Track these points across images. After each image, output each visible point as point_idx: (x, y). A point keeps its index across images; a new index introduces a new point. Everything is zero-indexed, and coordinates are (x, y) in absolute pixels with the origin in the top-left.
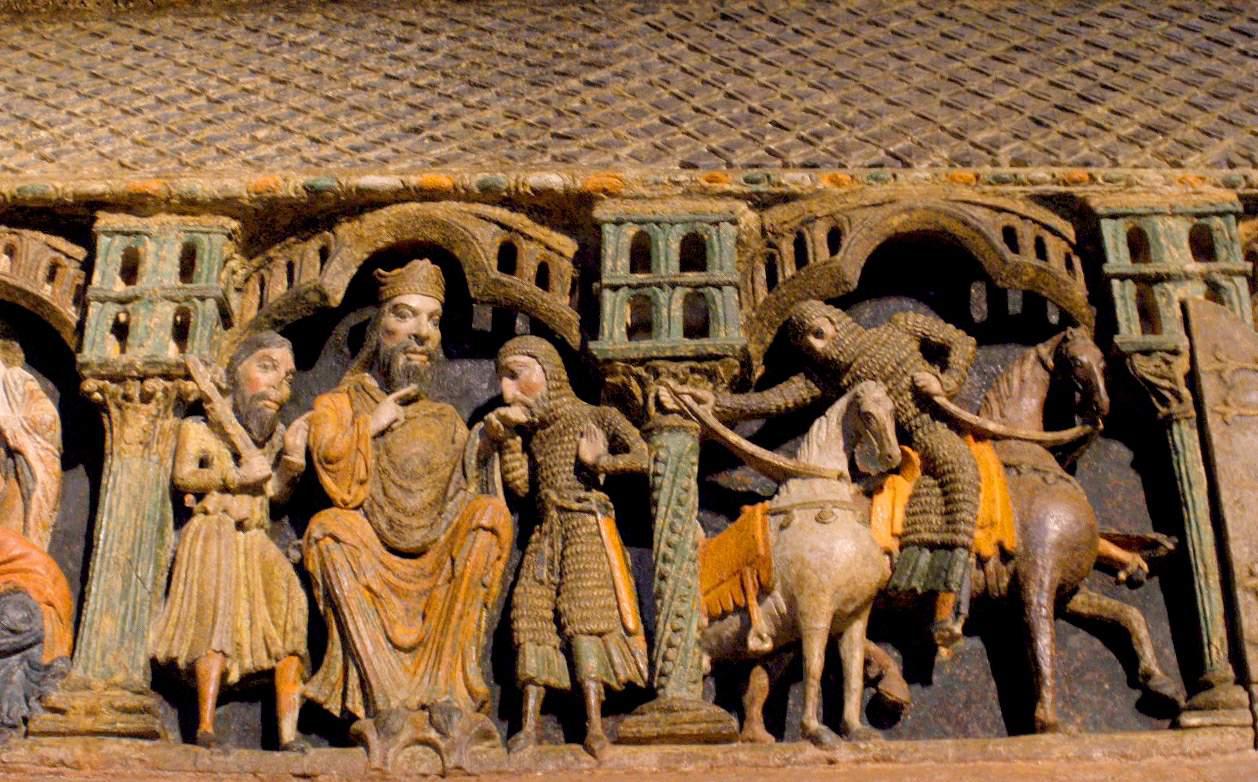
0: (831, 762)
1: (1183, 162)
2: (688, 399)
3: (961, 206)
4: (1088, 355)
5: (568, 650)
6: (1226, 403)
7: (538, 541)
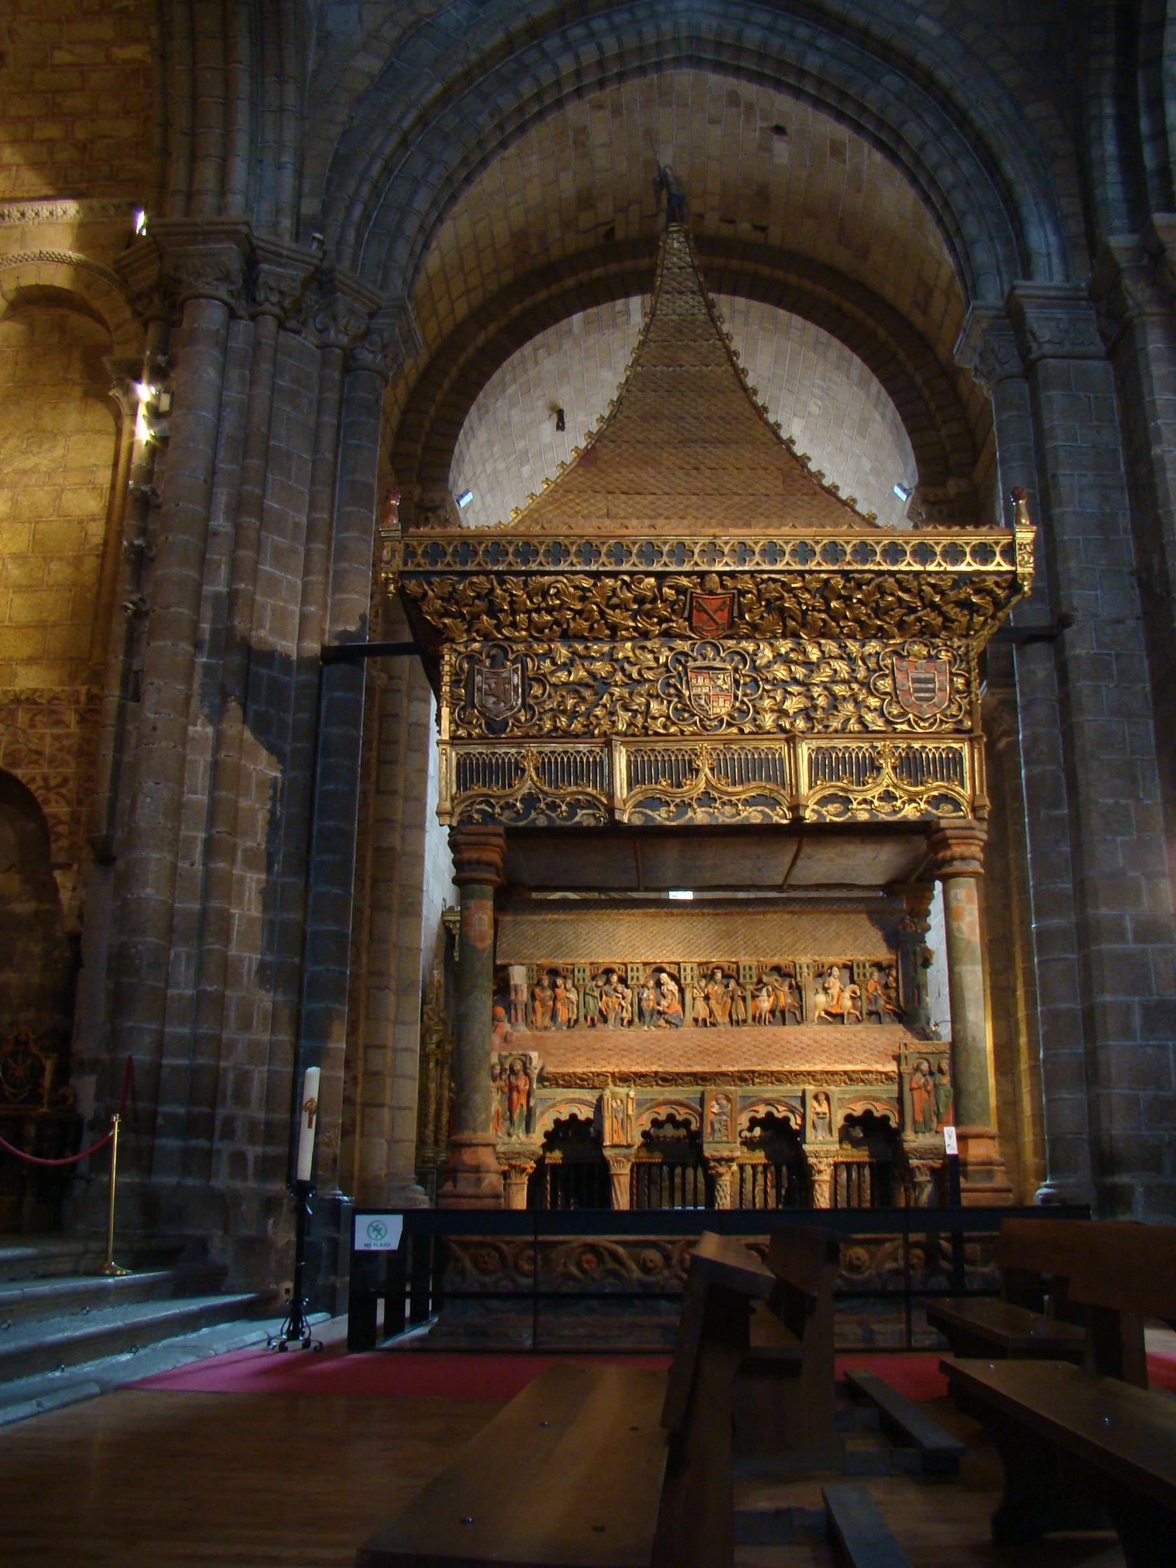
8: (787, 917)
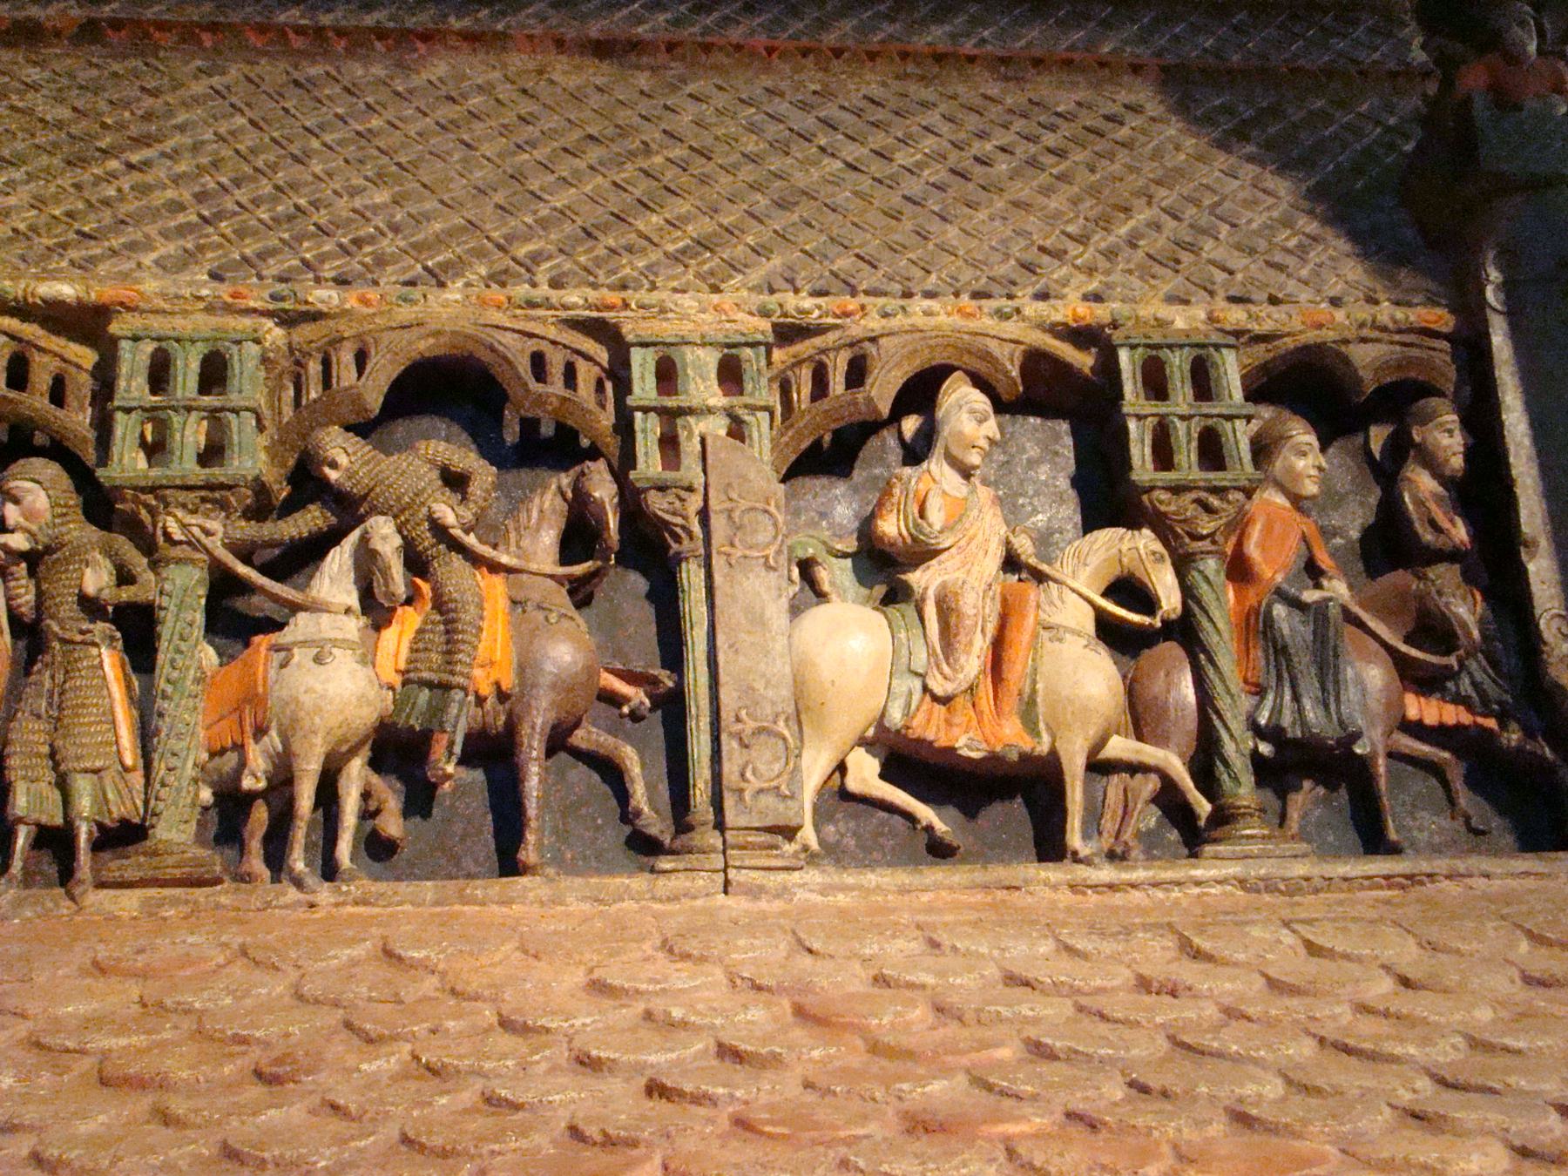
0: (312, 906)
1: (723, 286)
2: (196, 531)
3: (488, 330)
4: (603, 489)
5: (63, 784)
6: (732, 545)
7: (39, 672)
8: (566, 73)
